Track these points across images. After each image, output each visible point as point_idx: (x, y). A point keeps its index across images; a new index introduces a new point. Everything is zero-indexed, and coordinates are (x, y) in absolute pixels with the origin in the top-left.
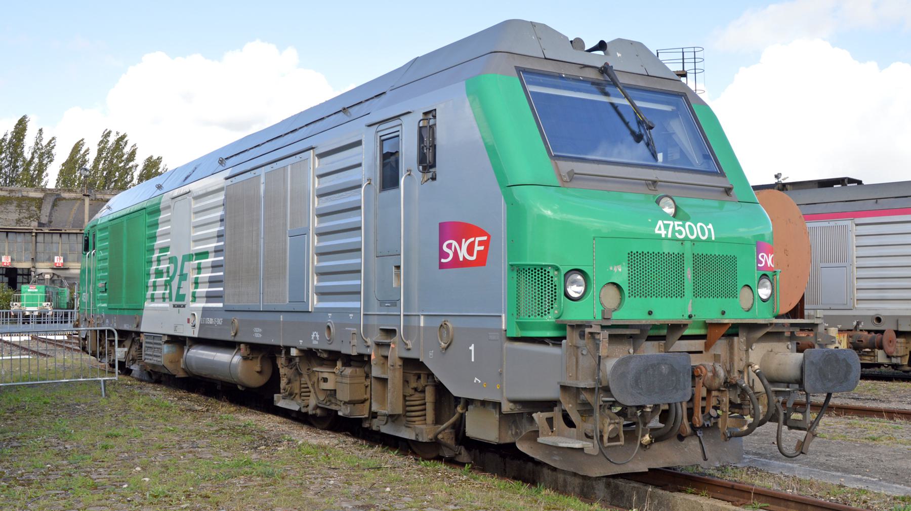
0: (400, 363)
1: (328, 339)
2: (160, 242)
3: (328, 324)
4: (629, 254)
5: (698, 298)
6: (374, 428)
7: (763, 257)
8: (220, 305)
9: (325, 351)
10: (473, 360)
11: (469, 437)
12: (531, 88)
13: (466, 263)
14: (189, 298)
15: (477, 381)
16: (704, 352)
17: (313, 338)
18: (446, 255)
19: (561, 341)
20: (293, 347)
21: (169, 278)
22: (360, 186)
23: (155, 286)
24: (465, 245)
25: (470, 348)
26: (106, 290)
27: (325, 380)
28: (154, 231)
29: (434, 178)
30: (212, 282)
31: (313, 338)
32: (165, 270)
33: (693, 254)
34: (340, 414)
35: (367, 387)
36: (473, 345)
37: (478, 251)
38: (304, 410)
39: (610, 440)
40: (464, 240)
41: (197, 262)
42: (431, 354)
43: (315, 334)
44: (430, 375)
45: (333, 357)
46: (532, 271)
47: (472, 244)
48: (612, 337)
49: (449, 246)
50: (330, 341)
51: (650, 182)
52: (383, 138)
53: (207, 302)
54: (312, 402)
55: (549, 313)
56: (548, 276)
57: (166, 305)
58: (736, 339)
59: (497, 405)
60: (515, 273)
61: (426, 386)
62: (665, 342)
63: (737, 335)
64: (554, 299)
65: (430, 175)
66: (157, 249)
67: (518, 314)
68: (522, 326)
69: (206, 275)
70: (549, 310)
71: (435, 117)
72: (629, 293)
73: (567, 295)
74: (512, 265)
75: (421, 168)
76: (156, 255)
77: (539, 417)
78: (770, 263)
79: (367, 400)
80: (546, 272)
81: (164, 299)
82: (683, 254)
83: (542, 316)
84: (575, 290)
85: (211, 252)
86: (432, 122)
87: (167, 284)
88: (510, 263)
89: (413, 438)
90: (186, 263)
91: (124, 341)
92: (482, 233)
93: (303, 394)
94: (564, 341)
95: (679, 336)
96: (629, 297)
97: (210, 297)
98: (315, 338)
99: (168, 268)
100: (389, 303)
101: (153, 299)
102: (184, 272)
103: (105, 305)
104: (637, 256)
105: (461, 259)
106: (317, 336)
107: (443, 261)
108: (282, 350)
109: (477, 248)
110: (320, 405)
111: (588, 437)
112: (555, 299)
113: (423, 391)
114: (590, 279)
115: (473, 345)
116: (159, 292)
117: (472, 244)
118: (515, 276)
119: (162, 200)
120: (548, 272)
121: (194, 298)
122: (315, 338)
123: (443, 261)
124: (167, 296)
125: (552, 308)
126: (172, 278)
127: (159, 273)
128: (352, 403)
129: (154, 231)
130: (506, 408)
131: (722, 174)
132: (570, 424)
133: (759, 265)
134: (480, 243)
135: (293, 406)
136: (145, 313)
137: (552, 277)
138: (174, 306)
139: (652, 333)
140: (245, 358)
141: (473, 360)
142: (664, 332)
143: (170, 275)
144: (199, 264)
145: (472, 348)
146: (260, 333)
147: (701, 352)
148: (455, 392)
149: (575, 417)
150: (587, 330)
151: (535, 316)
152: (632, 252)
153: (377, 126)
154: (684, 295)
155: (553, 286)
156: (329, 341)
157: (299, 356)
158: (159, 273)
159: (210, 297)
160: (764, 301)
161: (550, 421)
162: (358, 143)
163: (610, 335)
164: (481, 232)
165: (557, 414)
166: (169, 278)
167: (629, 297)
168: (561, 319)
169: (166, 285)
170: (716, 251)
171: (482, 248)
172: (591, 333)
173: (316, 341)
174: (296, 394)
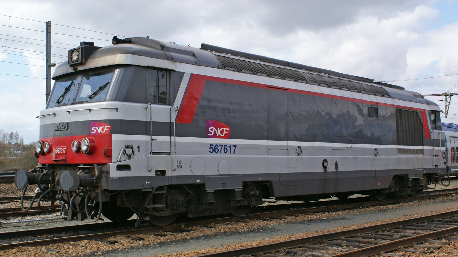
15: (198, 181)
24: (219, 130)
37: (225, 133)
40: (219, 128)
49: (212, 130)
109: (225, 132)
134: (226, 131)
171: (227, 132)
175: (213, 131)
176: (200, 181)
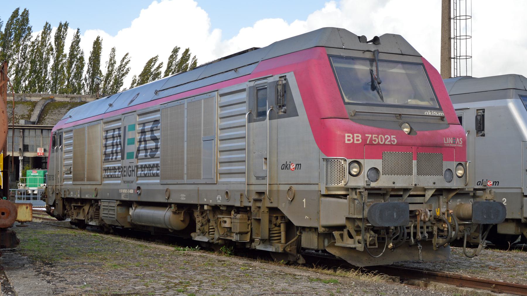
0: (267, 210)
1: (227, 199)
3: (227, 191)
5: (420, 175)
6: (253, 248)
9: (224, 206)
10: (305, 207)
17: (217, 199)
19: (347, 197)
20: (206, 205)
22: (245, 114)
25: (303, 201)
26: (71, 172)
27: (225, 222)
31: (217, 199)
34: (233, 240)
35: (248, 225)
36: (305, 199)
38: (212, 241)
39: (370, 245)
42: (283, 205)
43: (219, 197)
45: (229, 209)
48: (369, 194)
50: (228, 200)
51: (398, 115)
54: (217, 236)
55: (341, 182)
56: (341, 164)
58: (441, 197)
59: (316, 229)
60: (325, 163)
63: (442, 195)
68: (327, 189)
70: (341, 181)
72: (383, 173)
73: (350, 173)
77: (336, 234)
79: (249, 232)
86: (284, 82)
89: (274, 250)
91: (83, 206)
94: (348, 196)
95: (408, 195)
96: (383, 175)
98: (219, 199)
100: (260, 178)
103: (71, 182)
106: (220, 198)
110: (221, 238)
111: (359, 243)
113: (279, 226)
114: (362, 165)
115: (305, 199)
118: (325, 164)
120: (341, 162)
122: (219, 199)
125: (343, 180)
128: (241, 233)
130: (321, 230)
132: (351, 237)
135: (205, 239)
137: (343, 165)
139: (393, 193)
140: (174, 213)
141: (305, 207)
142: (401, 193)
145: (304, 200)
146: (184, 197)
147: (422, 203)
148: (296, 223)
149: (353, 233)
150: (358, 191)
156: (228, 200)
160: (459, 177)
161: (342, 236)
165: (345, 232)
167: (383, 175)
168: (347, 185)
172: (360, 192)
173: (219, 200)
174: (206, 232)
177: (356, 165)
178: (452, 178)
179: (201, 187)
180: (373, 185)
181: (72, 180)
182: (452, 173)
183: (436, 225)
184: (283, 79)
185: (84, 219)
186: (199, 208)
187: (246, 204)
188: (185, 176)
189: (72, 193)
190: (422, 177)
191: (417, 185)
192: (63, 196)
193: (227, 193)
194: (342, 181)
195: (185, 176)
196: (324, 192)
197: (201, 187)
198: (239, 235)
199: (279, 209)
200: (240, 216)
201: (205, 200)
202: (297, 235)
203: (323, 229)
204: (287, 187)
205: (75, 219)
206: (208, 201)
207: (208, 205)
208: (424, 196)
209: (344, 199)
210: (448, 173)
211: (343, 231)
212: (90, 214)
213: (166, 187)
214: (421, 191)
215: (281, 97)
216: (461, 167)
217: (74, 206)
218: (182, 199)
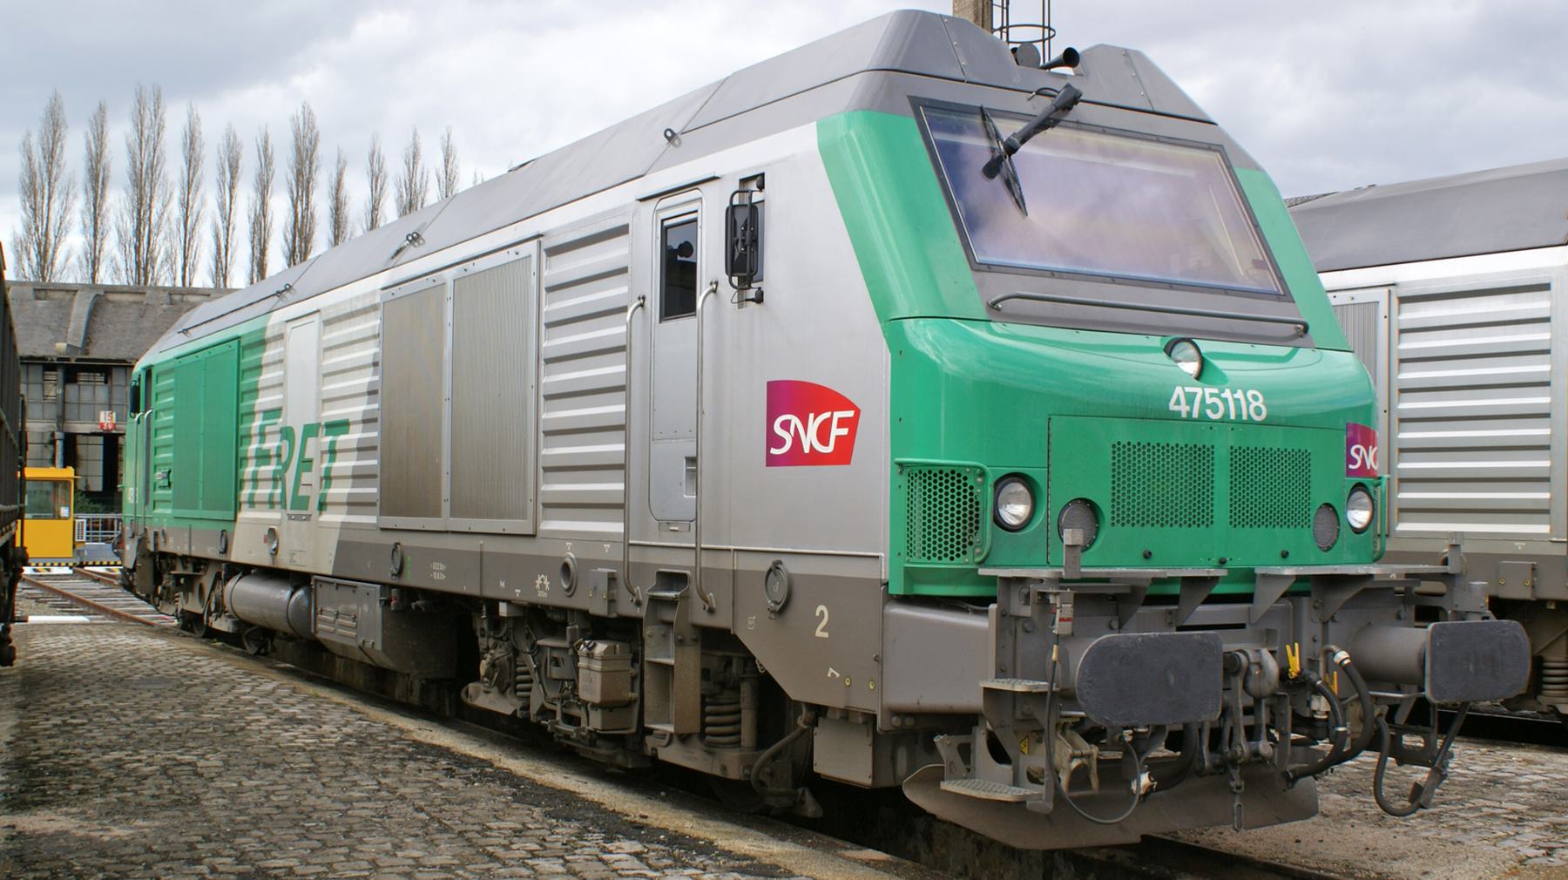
2: (264, 401)
3: (568, 560)
4: (1114, 446)
6: (649, 752)
7: (1357, 451)
8: (372, 519)
11: (819, 774)
12: (936, 136)
13: (815, 458)
14: (314, 504)
15: (832, 674)
16: (1248, 626)
17: (538, 586)
18: (780, 442)
19: (988, 606)
20: (503, 601)
21: (280, 467)
23: (255, 480)
24: (814, 424)
26: (169, 484)
28: (254, 380)
29: (759, 299)
30: (358, 477)
31: (538, 586)
32: (273, 452)
33: (1232, 448)
37: (838, 438)
39: (1072, 785)
40: (812, 416)
41: (330, 438)
42: (750, 623)
43: (542, 580)
44: (749, 659)
46: (935, 475)
47: (828, 423)
48: (1081, 600)
49: (786, 425)
50: (571, 591)
52: (666, 223)
53: (349, 513)
56: (965, 485)
57: (275, 515)
58: (1305, 601)
61: (743, 679)
62: (1176, 607)
63: (1307, 594)
64: (975, 524)
65: (752, 294)
66: (259, 412)
67: (910, 552)
69: (345, 464)
70: (964, 546)
71: (761, 187)
72: (1113, 518)
73: (998, 521)
74: (900, 464)
75: (735, 280)
76: (257, 423)
78: (1369, 462)
80: (961, 478)
81: (271, 503)
82: (1213, 447)
83: (952, 559)
84: (1015, 511)
85: (355, 423)
86: (756, 197)
87: (276, 479)
88: (897, 459)
89: (717, 772)
90: (311, 441)
92: (846, 404)
93: (519, 686)
94: (993, 607)
95: (1204, 596)
96: (1113, 524)
97: (354, 504)
98: (542, 586)
99: (279, 448)
101: (252, 503)
102: (307, 456)
103: (169, 511)
104: (1129, 450)
105: (807, 450)
106: (547, 583)
107: (774, 451)
108: (481, 605)
109: (836, 432)
111: (1034, 779)
112: (977, 528)
113: (737, 689)
116: (264, 491)
117: (828, 423)
119: (270, 323)
120: (965, 478)
121: (322, 506)
122: (542, 586)
123: (774, 451)
124: (277, 499)
126: (286, 466)
127: (263, 457)
129: (254, 380)
131: (1285, 296)
133: (1351, 467)
134: (842, 423)
135: (505, 706)
136: (238, 526)
137: (971, 488)
138: (290, 516)
142: (1176, 589)
143: (284, 459)
144: (333, 443)
147: (1242, 626)
148: (795, 689)
151: (940, 558)
152: (1119, 443)
153: (657, 199)
154: (1212, 522)
155: (973, 503)
156: (568, 590)
157: (515, 618)
158: (263, 457)
159: (354, 504)
160: (1357, 531)
162: (622, 230)
163: (1076, 596)
164: (842, 403)
166: (280, 467)
169: (275, 480)
170: (1276, 440)
171: (844, 431)
172: (1044, 595)
173: (544, 589)
175: (789, 431)
176: (838, 675)
177: (1020, 488)
178: (1338, 536)
179: (492, 546)
180: (1093, 565)
181: (171, 504)
182: (1336, 521)
183: (1288, 699)
184: (753, 186)
185: (199, 609)
186: (484, 609)
187: (627, 608)
188: (446, 507)
189: (171, 540)
190: (1248, 535)
191: (1229, 562)
192: (151, 548)
193: (566, 567)
194: (969, 548)
195: (446, 507)
196: (897, 589)
197: (492, 546)
198: (599, 710)
199: (735, 638)
200: (605, 652)
201: (502, 584)
202: (796, 725)
203: (896, 721)
204: (765, 564)
205: (182, 610)
206: (508, 590)
207: (508, 602)
208: (1247, 598)
209: (976, 612)
210: (1326, 517)
211: (969, 732)
212: (213, 600)
213: (390, 539)
214: (1244, 582)
215: (745, 247)
216: (1359, 494)
217: (178, 577)
218: (436, 576)
